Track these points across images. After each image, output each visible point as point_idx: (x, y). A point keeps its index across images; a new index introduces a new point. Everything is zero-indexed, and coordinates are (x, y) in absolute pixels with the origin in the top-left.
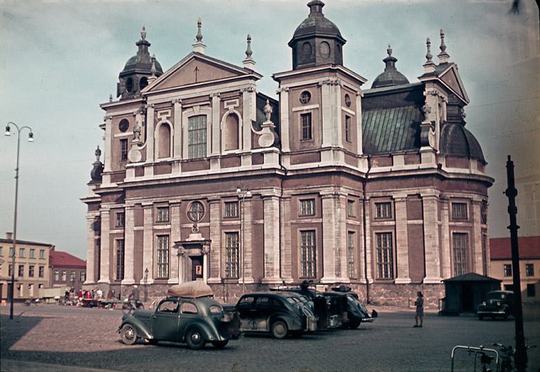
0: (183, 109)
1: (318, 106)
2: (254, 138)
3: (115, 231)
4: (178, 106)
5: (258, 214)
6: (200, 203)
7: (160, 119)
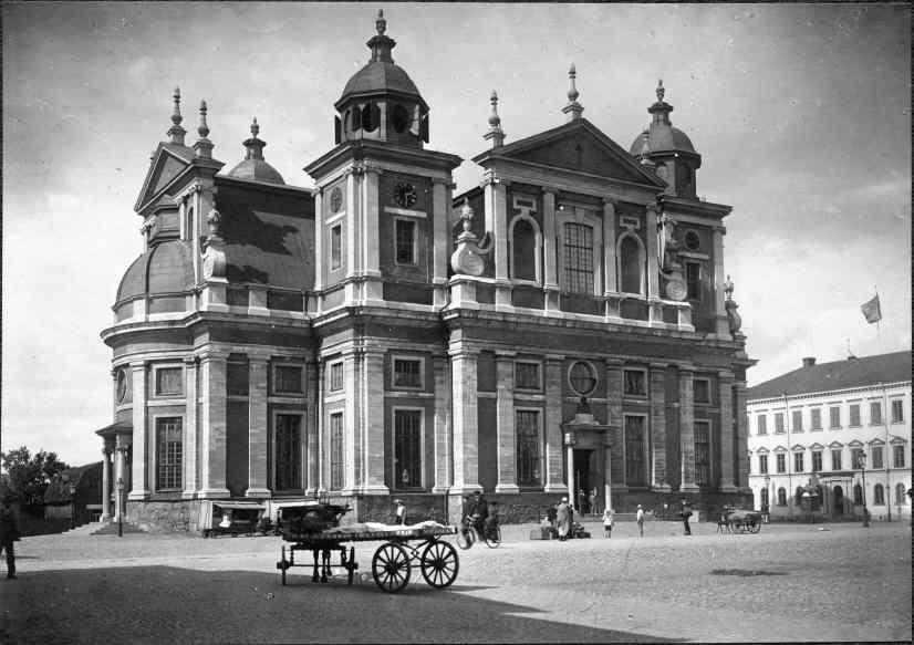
1: (706, 257)
2: (663, 282)
3: (397, 394)
4: (549, 199)
5: (674, 395)
6: (589, 368)
7: (519, 211)
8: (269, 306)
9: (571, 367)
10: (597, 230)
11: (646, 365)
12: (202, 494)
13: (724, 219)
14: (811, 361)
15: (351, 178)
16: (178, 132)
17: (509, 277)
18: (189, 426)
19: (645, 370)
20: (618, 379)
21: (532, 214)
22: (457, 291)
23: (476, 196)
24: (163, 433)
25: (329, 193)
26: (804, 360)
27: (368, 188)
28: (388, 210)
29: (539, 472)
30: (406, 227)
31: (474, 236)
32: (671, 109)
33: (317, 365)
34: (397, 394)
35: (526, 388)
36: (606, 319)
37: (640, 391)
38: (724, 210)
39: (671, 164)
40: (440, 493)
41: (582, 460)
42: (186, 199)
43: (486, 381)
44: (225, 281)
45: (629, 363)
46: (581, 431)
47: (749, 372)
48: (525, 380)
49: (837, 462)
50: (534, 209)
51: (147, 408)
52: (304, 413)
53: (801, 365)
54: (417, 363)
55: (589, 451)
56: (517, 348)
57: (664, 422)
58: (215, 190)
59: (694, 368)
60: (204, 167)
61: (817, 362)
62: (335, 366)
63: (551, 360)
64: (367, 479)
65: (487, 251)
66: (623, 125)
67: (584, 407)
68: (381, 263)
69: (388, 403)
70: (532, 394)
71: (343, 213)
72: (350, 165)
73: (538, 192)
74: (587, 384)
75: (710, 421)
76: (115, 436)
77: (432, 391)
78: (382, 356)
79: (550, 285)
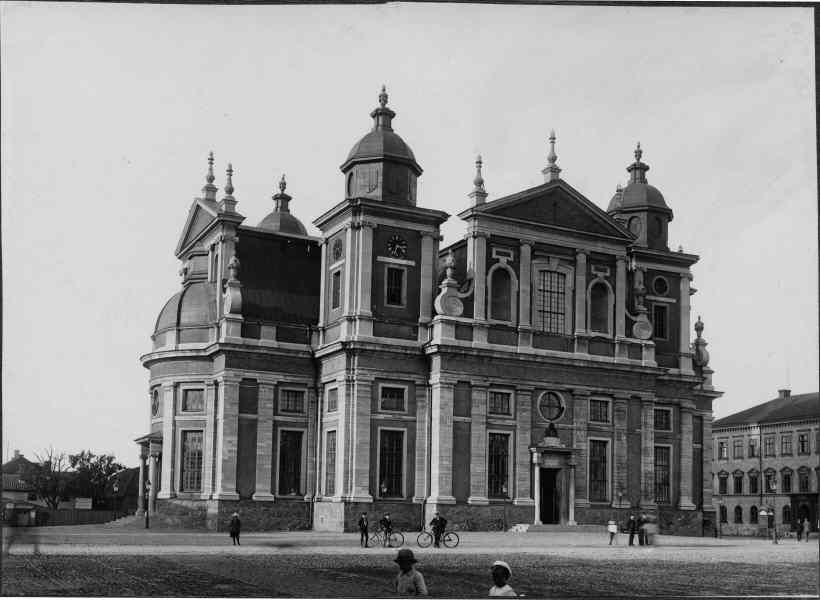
0: (533, 256)
2: (629, 324)
4: (526, 250)
7: (498, 261)
8: (278, 339)
9: (540, 398)
10: (570, 277)
11: (611, 396)
12: (216, 497)
13: (692, 268)
14: (786, 393)
15: (349, 230)
16: (211, 189)
17: (486, 318)
18: (208, 440)
19: (610, 400)
20: (584, 408)
21: (509, 262)
22: (438, 329)
23: (460, 247)
24: (186, 444)
25: (332, 243)
26: (780, 392)
27: (364, 239)
28: (380, 259)
29: (507, 487)
30: (395, 274)
31: (455, 282)
32: (647, 168)
33: (317, 389)
34: (381, 417)
35: (497, 414)
36: (577, 355)
37: (604, 418)
38: (689, 260)
39: (643, 216)
40: (418, 502)
41: (549, 477)
43: (461, 406)
44: (240, 317)
45: (594, 393)
46: (547, 453)
47: (715, 402)
48: (499, 405)
49: (805, 484)
50: (511, 259)
51: (174, 422)
52: (305, 430)
53: (776, 396)
55: (556, 471)
56: (491, 379)
57: (626, 446)
58: (237, 239)
59: (655, 400)
60: (230, 220)
61: (792, 394)
62: (331, 390)
63: (521, 390)
64: (354, 488)
65: (468, 294)
66: (600, 187)
67: (552, 431)
68: (372, 305)
69: (374, 424)
72: (348, 220)
73: (516, 245)
74: (556, 411)
75: (671, 446)
76: (150, 444)
77: (414, 414)
78: (370, 384)
79: (524, 324)
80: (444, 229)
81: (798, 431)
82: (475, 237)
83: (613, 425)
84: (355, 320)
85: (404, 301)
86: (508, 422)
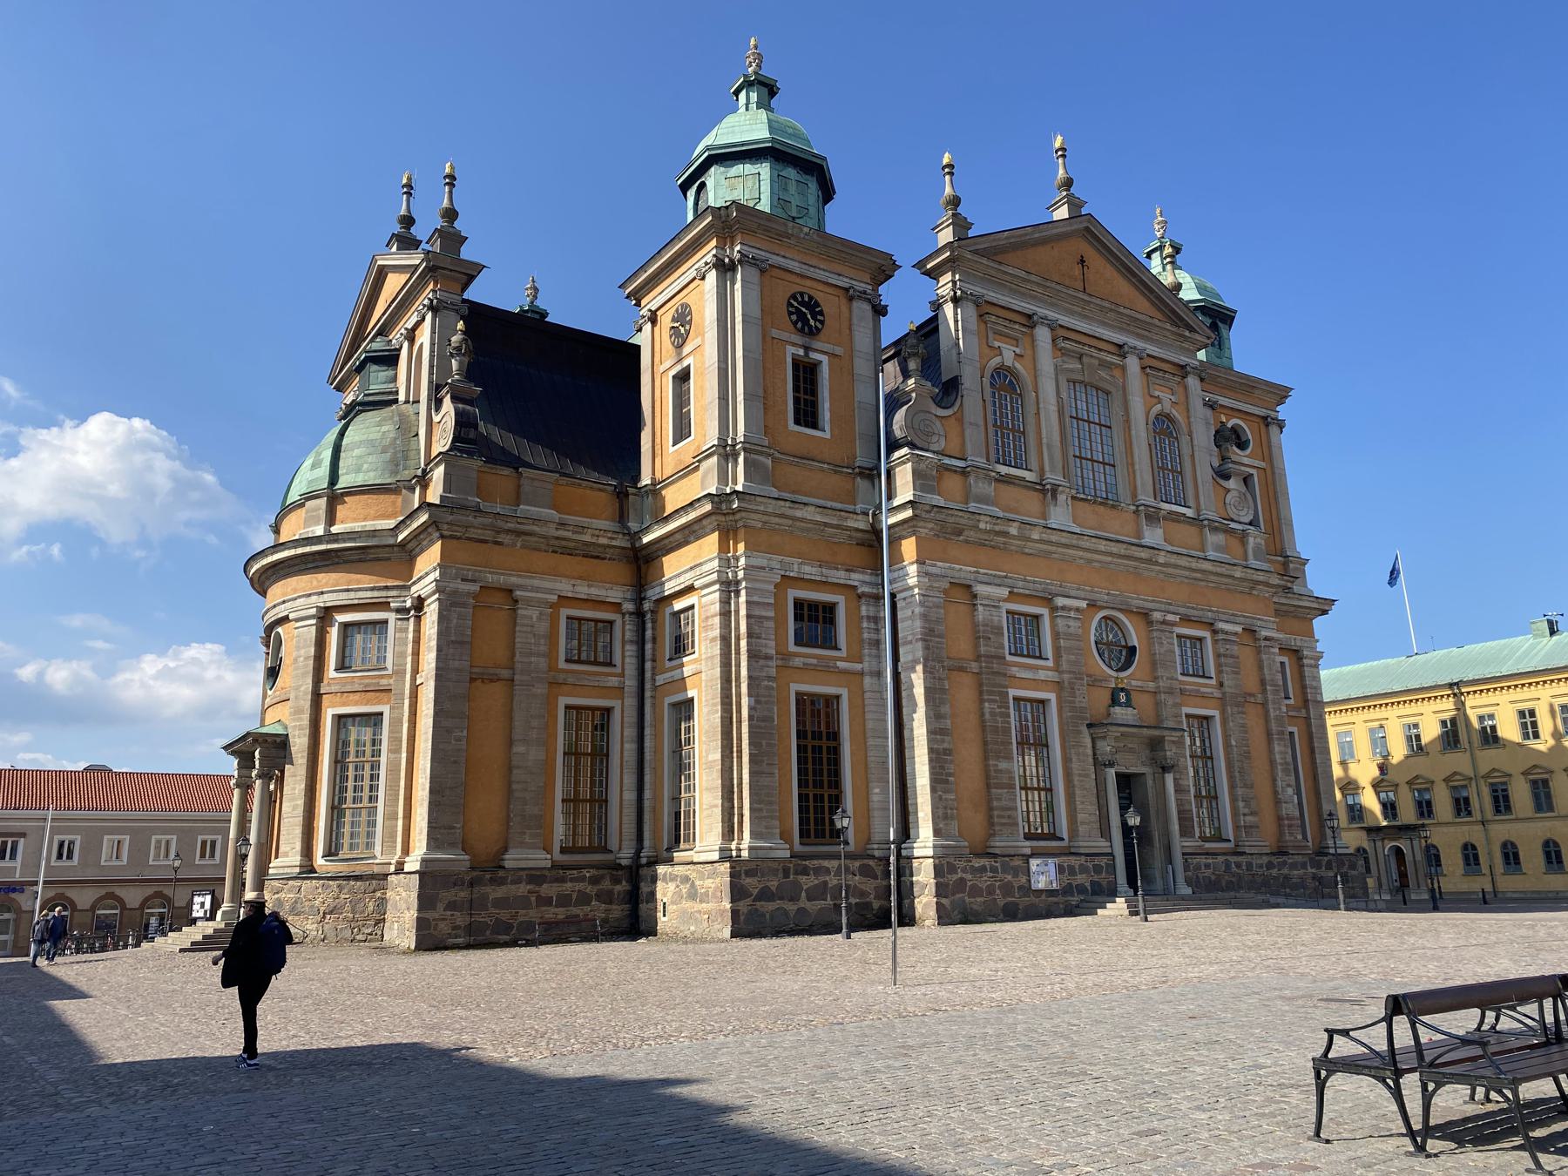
4: (1043, 334)
11: (1210, 625)
25: (666, 320)
38: (1282, 394)
42: (411, 336)
54: (830, 609)
63: (1063, 608)
70: (1037, 668)
71: (698, 341)
78: (771, 588)
80: (888, 293)
81: (1366, 721)
82: (956, 300)
83: (1221, 685)
84: (735, 456)
85: (827, 428)
86: (1042, 675)
